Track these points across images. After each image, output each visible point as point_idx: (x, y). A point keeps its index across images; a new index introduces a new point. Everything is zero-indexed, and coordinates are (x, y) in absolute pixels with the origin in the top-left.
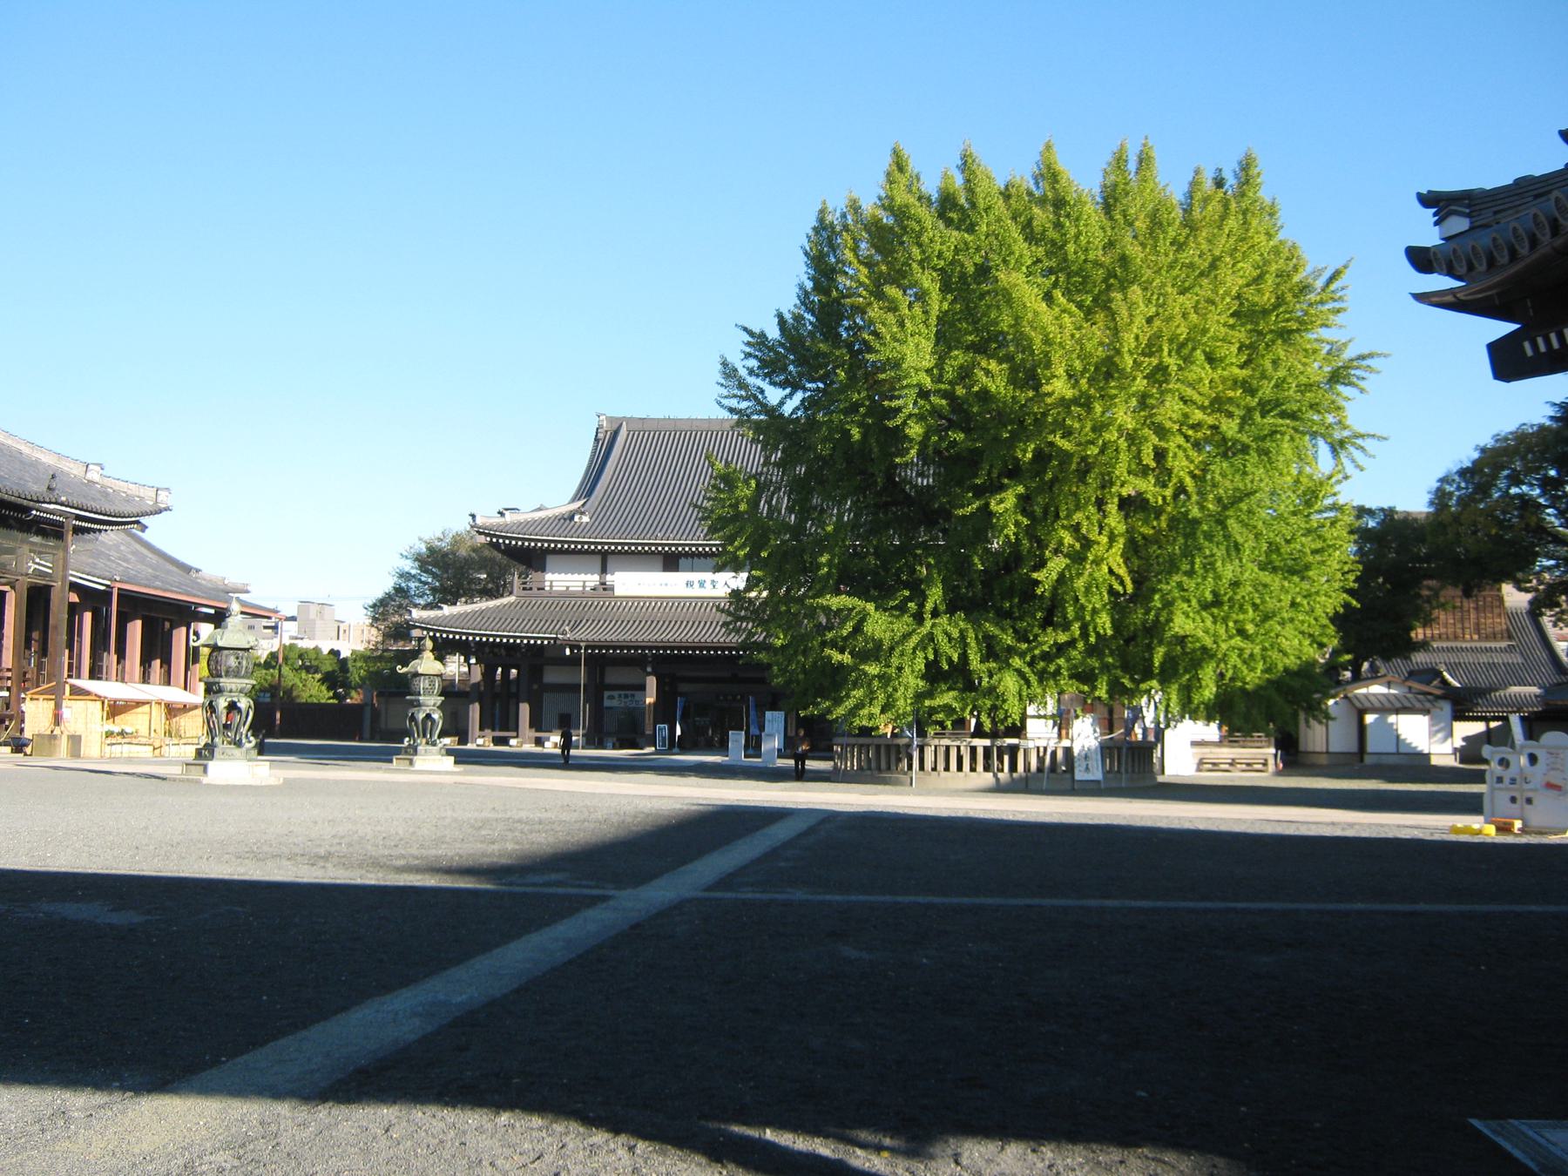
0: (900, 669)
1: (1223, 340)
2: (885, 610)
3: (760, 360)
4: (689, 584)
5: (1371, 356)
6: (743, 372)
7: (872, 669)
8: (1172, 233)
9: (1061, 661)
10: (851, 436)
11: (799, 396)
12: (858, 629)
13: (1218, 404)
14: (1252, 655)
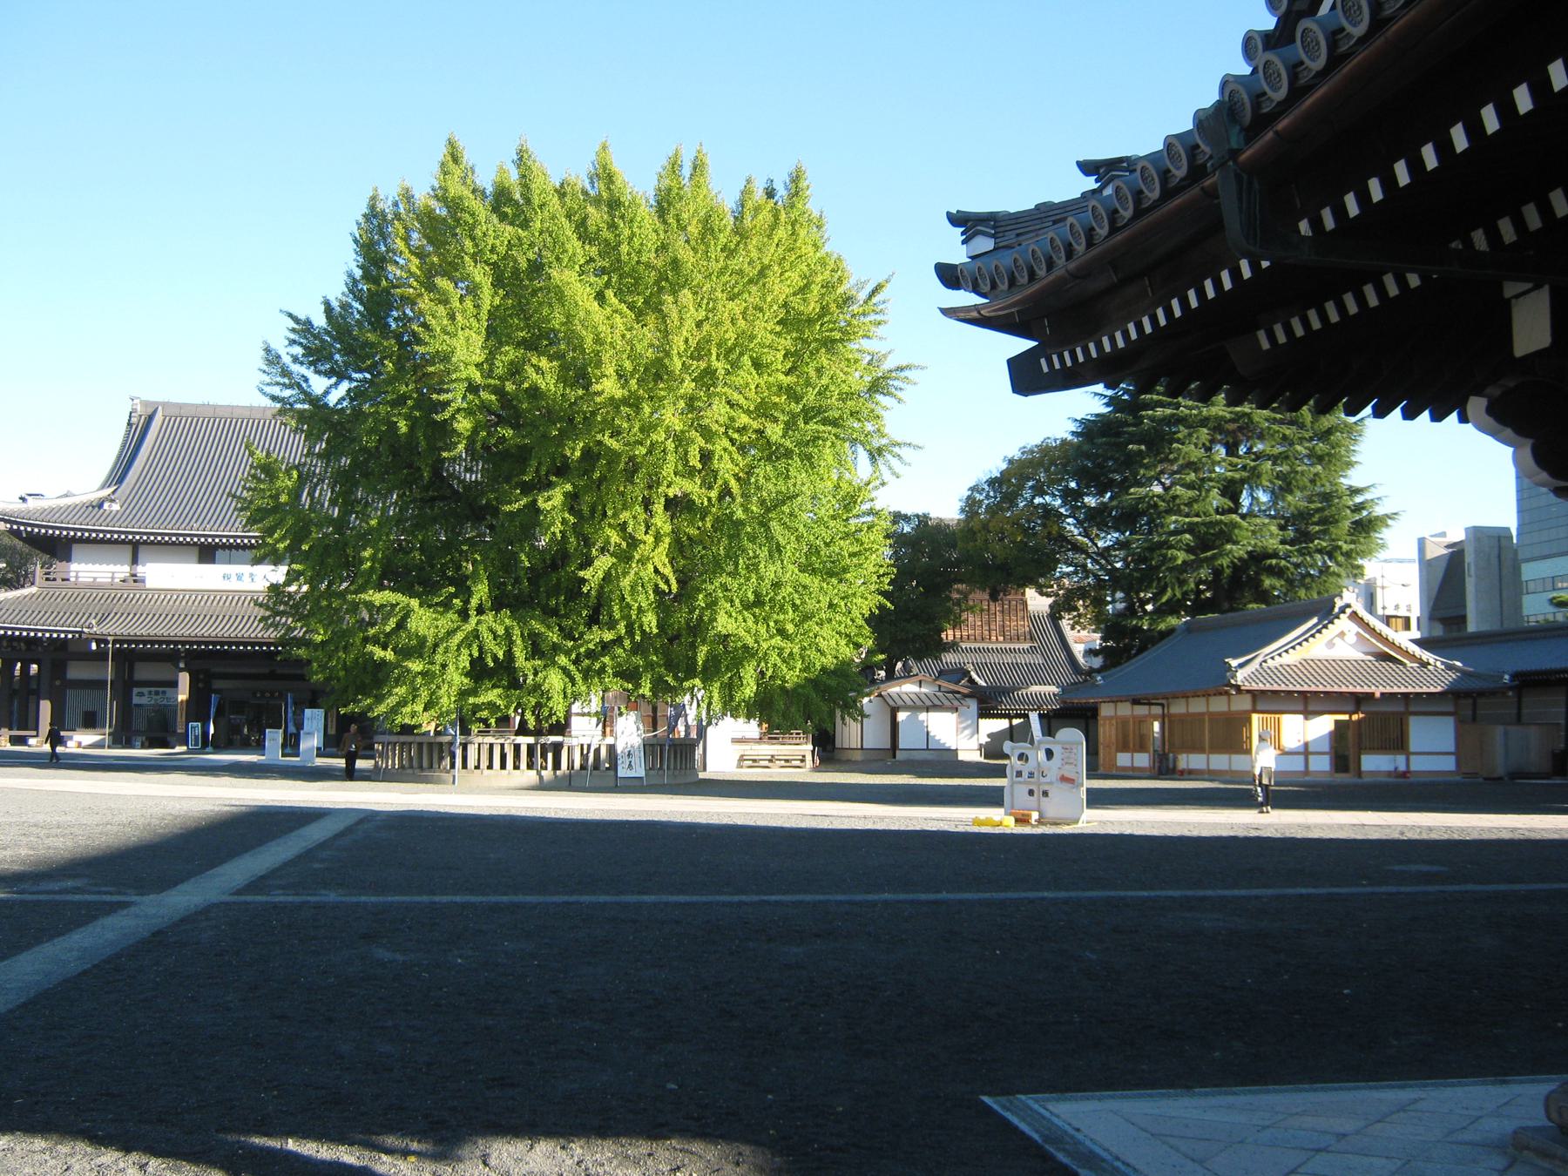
0: (444, 666)
1: (770, 347)
2: (430, 606)
3: (305, 348)
4: (226, 577)
5: (908, 367)
6: (287, 360)
7: (416, 666)
8: (723, 240)
9: (606, 659)
10: (398, 428)
11: (345, 386)
12: (401, 625)
13: (763, 410)
14: (791, 654)
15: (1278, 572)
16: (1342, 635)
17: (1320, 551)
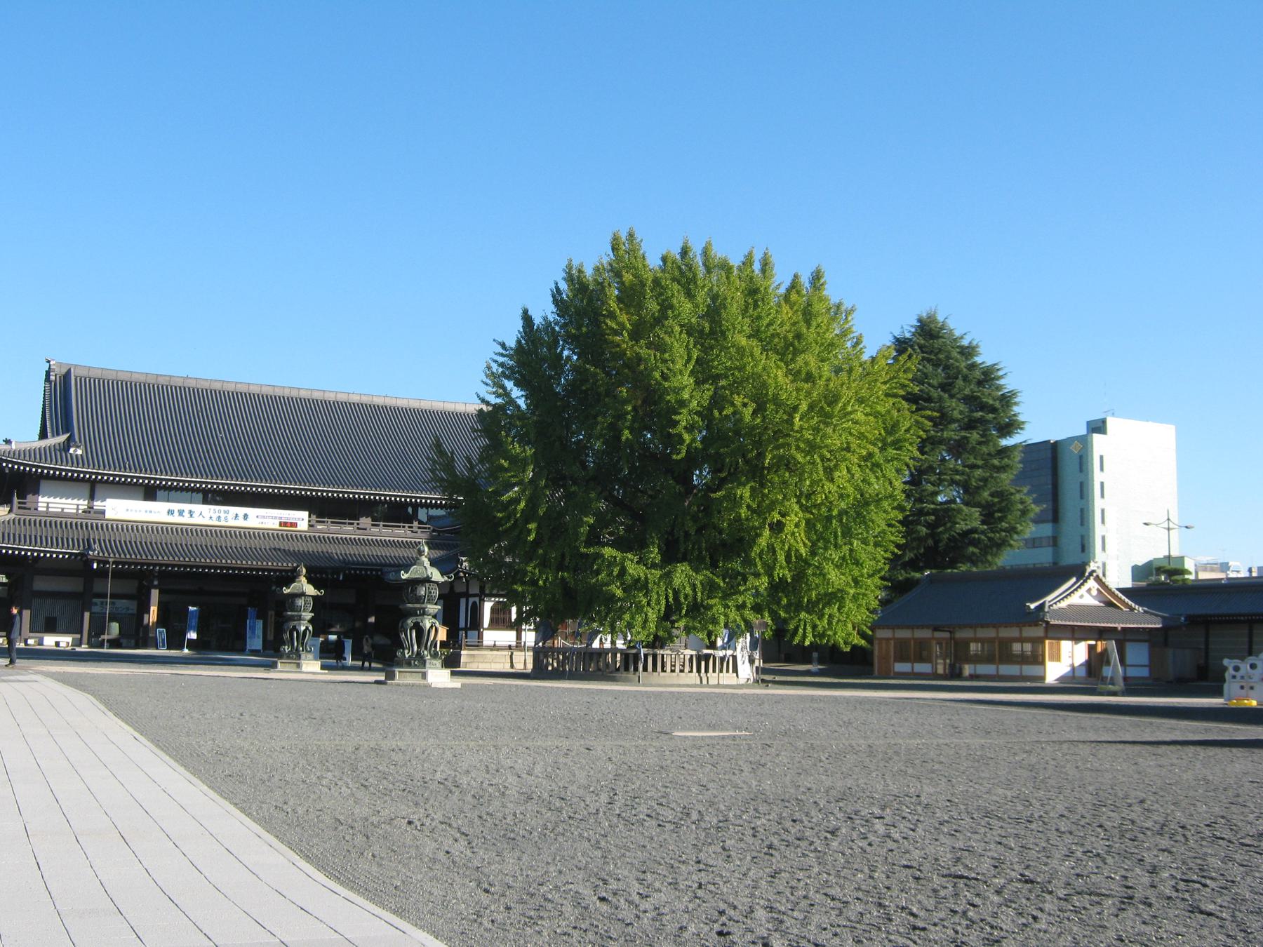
4: (171, 512)
15: (975, 543)
16: (1089, 591)
17: (1002, 530)
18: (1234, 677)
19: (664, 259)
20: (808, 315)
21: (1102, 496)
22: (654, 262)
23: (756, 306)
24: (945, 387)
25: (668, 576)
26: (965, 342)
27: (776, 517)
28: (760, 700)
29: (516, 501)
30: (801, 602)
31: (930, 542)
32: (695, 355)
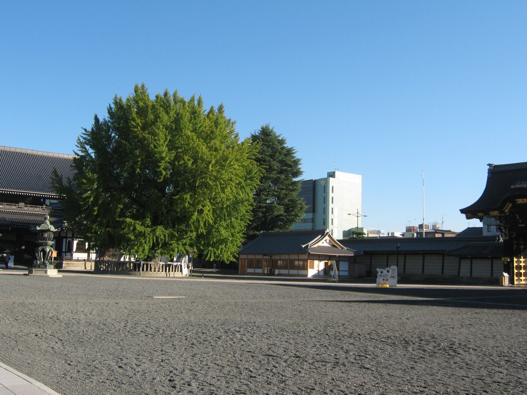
15: (282, 220)
16: (326, 240)
18: (381, 276)
19: (157, 97)
20: (216, 123)
21: (332, 203)
22: (152, 98)
23: (195, 119)
24: (271, 156)
25: (154, 231)
26: (280, 138)
27: (200, 207)
28: (191, 283)
29: (89, 197)
30: (209, 243)
31: (263, 219)
32: (169, 138)
